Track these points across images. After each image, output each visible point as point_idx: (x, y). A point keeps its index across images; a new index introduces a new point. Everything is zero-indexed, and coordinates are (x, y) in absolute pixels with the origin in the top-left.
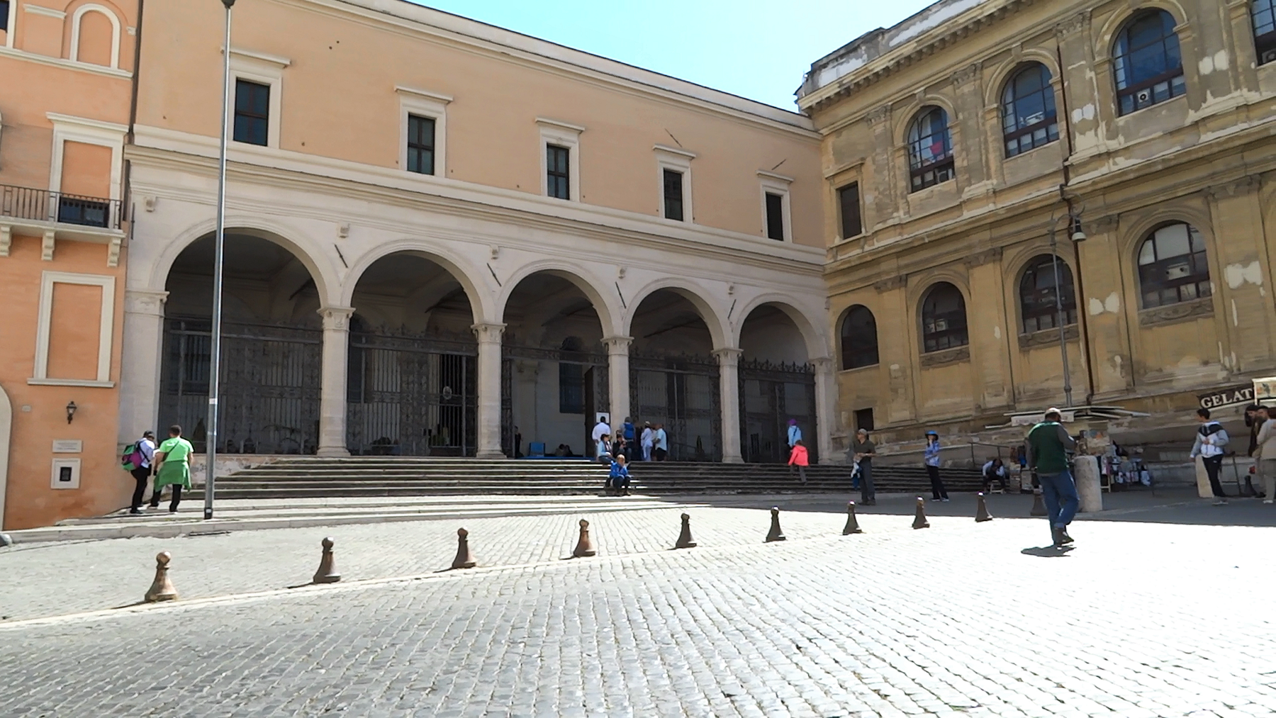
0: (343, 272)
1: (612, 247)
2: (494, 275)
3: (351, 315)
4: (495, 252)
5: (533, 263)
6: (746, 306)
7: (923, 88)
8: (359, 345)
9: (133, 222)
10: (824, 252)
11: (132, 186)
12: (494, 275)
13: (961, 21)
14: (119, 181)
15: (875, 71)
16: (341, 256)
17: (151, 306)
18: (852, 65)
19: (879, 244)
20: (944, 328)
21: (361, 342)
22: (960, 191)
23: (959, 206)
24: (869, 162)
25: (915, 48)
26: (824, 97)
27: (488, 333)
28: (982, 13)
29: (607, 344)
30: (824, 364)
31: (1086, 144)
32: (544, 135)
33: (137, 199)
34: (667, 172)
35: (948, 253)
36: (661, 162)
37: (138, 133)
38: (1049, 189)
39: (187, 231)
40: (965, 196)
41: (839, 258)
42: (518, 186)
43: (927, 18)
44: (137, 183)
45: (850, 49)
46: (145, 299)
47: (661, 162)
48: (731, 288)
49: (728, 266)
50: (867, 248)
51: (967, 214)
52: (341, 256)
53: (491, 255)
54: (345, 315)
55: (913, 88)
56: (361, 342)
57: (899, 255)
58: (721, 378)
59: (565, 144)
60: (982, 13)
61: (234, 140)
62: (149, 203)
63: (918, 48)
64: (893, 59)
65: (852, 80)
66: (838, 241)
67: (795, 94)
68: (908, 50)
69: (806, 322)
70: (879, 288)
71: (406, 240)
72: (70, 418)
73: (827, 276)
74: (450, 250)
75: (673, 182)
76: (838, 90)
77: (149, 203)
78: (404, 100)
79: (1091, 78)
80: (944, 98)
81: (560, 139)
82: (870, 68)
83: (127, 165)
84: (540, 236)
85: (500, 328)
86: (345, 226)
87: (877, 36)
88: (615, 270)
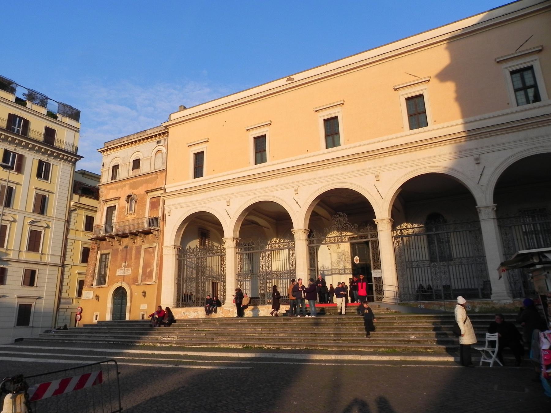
1: (369, 164)
2: (297, 203)
6: (496, 169)
12: (297, 203)
16: (228, 214)
33: (166, 212)
37: (167, 188)
46: (168, 249)
47: (402, 95)
48: (477, 159)
54: (230, 240)
62: (169, 213)
71: (255, 198)
72: (145, 296)
74: (275, 197)
81: (330, 114)
84: (321, 173)
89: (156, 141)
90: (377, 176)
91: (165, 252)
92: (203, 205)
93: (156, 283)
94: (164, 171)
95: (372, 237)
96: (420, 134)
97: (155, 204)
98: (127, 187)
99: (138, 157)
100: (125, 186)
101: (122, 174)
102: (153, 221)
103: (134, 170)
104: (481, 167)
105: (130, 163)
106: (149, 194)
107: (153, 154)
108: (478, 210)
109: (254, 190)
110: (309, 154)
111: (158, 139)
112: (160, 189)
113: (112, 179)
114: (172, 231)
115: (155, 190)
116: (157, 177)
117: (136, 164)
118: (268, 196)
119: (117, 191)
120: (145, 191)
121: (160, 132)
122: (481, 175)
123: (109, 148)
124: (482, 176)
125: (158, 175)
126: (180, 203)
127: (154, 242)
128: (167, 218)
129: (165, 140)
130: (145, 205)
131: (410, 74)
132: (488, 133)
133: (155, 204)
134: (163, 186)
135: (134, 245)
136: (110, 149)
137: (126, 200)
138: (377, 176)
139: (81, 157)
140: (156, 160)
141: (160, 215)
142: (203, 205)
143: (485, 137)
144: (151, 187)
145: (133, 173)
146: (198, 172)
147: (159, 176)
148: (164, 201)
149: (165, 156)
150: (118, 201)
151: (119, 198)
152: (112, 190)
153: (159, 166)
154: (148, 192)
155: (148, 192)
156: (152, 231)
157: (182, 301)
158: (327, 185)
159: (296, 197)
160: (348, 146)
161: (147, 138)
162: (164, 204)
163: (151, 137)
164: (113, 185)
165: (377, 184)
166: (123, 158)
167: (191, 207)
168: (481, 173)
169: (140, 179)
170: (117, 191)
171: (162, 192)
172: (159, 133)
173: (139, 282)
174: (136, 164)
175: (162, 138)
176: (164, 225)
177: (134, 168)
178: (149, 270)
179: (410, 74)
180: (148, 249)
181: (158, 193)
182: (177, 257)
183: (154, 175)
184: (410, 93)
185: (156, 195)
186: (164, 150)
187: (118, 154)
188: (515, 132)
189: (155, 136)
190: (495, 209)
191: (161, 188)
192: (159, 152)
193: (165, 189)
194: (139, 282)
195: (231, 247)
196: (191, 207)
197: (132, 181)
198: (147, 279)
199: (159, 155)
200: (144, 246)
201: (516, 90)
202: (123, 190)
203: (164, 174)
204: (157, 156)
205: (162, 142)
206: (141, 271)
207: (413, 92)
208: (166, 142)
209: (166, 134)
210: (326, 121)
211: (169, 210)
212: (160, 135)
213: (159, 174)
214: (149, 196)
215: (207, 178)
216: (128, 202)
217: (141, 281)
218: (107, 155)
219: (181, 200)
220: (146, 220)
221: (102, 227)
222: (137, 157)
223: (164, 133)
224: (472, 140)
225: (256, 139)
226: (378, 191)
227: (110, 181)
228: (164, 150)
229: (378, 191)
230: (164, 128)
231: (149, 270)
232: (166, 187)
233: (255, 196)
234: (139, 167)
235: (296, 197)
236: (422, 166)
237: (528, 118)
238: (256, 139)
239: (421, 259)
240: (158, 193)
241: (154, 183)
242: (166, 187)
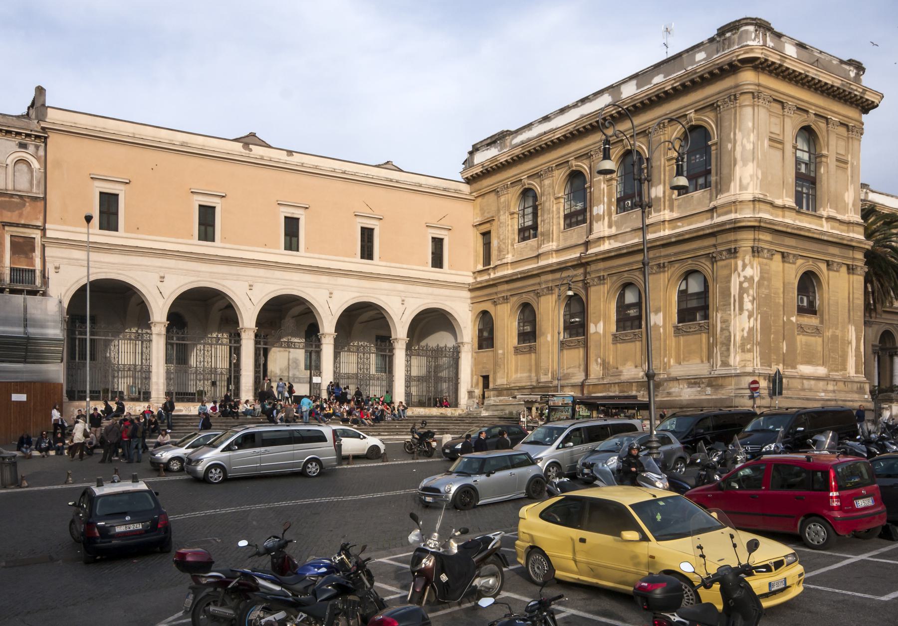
0: (161, 302)
1: (324, 279)
3: (167, 326)
4: (250, 286)
7: (526, 176)
8: (172, 341)
9: (48, 278)
10: (472, 274)
11: (46, 258)
13: (543, 139)
14: (40, 257)
15: (501, 161)
16: (161, 293)
18: (493, 152)
19: (500, 273)
20: (529, 330)
21: (173, 340)
22: (539, 247)
23: (538, 257)
24: (496, 220)
25: (521, 151)
26: (475, 173)
27: (247, 333)
28: (554, 136)
29: (321, 337)
31: (601, 229)
32: (282, 212)
33: (50, 267)
34: (363, 229)
35: (529, 286)
36: (359, 223)
38: (575, 254)
40: (541, 251)
41: (479, 279)
43: (531, 130)
44: (48, 257)
45: (492, 141)
49: (400, 286)
50: (492, 276)
51: (543, 262)
52: (161, 293)
55: (521, 175)
56: (173, 340)
57: (507, 282)
58: (394, 356)
60: (554, 136)
61: (100, 229)
62: (57, 268)
63: (523, 151)
64: (509, 156)
65: (488, 165)
66: (480, 267)
67: (463, 164)
68: (518, 151)
69: (455, 319)
70: (495, 303)
73: (471, 290)
74: (224, 286)
75: (367, 235)
76: (482, 169)
77: (56, 268)
78: (196, 197)
79: (604, 189)
80: (535, 184)
81: (293, 213)
82: (498, 159)
83: (44, 247)
84: (278, 274)
87: (505, 136)
90: (331, 293)
97: (23, 247)
104: (404, 306)
106: (7, 228)
107: (10, 161)
109: (199, 271)
111: (22, 139)
112: (37, 227)
115: (25, 226)
116: (24, 205)
118: (216, 283)
121: (33, 133)
125: (25, 201)
129: (37, 147)
133: (23, 247)
134: (39, 223)
138: (331, 293)
147: (27, 204)
159: (249, 292)
160: (308, 255)
165: (329, 300)
172: (29, 132)
175: (32, 144)
183: (16, 200)
185: (23, 233)
186: (35, 164)
189: (19, 134)
193: (44, 230)
199: (23, 167)
203: (41, 204)
205: (31, 149)
207: (367, 224)
212: (28, 135)
213: (27, 200)
223: (37, 137)
228: (35, 164)
230: (39, 129)
233: (199, 279)
235: (249, 292)
239: (123, 363)
241: (17, 213)
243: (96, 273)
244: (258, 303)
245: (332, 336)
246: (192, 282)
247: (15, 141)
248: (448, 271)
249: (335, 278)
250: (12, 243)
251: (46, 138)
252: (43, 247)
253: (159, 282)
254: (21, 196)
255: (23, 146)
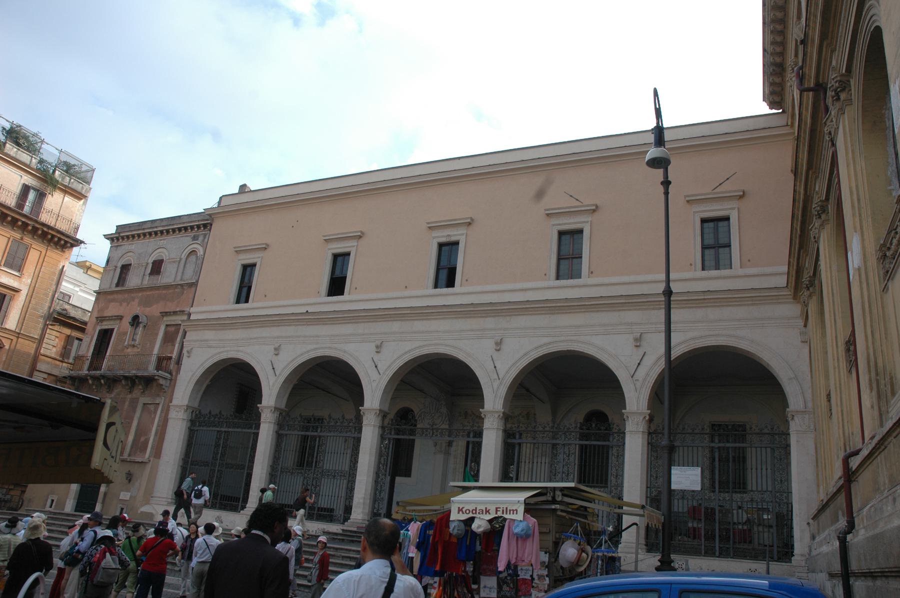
0: (272, 379)
1: (489, 322)
2: (376, 367)
5: (410, 351)
9: (181, 364)
12: (376, 367)
16: (273, 369)
17: (180, 413)
30: (795, 418)
33: (185, 351)
36: (554, 225)
39: (202, 365)
42: (406, 287)
53: (374, 349)
54: (270, 410)
59: (454, 239)
62: (188, 352)
71: (316, 349)
81: (449, 236)
84: (419, 325)
85: (375, 411)
86: (277, 346)
88: (489, 344)
89: (192, 235)
91: (173, 414)
92: (241, 348)
93: (150, 461)
94: (194, 285)
95: (474, 437)
96: (569, 290)
98: (137, 301)
99: (161, 255)
100: (133, 299)
101: (134, 280)
102: (162, 362)
103: (152, 277)
105: (148, 265)
106: (165, 319)
107: (184, 256)
108: (625, 417)
109: (318, 336)
110: (407, 293)
113: (117, 285)
114: (188, 383)
115: (175, 313)
116: (183, 293)
117: (157, 267)
119: (121, 305)
120: (161, 313)
122: (639, 364)
123: (121, 235)
124: (640, 366)
125: (184, 289)
126: (207, 340)
127: (158, 395)
128: (185, 361)
130: (157, 334)
131: (571, 196)
132: (658, 303)
134: (187, 309)
135: (129, 396)
136: (123, 238)
137: (130, 323)
139: (82, 242)
140: (187, 266)
141: (174, 355)
142: (241, 348)
143: (653, 309)
144: (171, 307)
145: (149, 279)
146: (244, 293)
147: (185, 292)
148: (186, 332)
149: (199, 262)
150: (118, 322)
151: (120, 318)
152: (113, 303)
153: (189, 277)
154: (165, 314)
155: (165, 314)
156: (157, 377)
157: (221, 500)
158: (424, 346)
161: (180, 229)
162: (184, 338)
163: (186, 229)
164: (115, 296)
166: (139, 254)
167: (222, 350)
168: (639, 362)
169: (157, 292)
170: (121, 305)
171: (185, 318)
173: (125, 456)
174: (157, 267)
175: (202, 232)
176: (178, 370)
177: (151, 274)
178: (142, 439)
179: (571, 196)
180: (148, 406)
181: (177, 319)
182: (189, 424)
184: (565, 224)
185: (174, 321)
186: (201, 252)
187: (133, 247)
188: (692, 307)
189: (192, 228)
190: (647, 418)
191: (184, 311)
192: (193, 253)
193: (189, 315)
194: (125, 456)
195: (268, 421)
196: (222, 350)
197: (145, 293)
198: (138, 453)
199: (193, 258)
200: (143, 400)
201: (704, 247)
202: (129, 305)
203: (193, 289)
204: (190, 259)
205: (201, 238)
206: (131, 438)
208: (206, 240)
209: (208, 228)
210: (441, 245)
211: (189, 349)
212: (199, 227)
214: (164, 321)
215: (256, 306)
216: (132, 325)
217: (129, 455)
218: (117, 246)
219: (209, 335)
220: (154, 359)
221: (88, 359)
222: (159, 256)
223: (205, 226)
224: (635, 310)
225: (336, 256)
226: (495, 367)
227: (114, 288)
229: (495, 367)
231: (142, 439)
232: (192, 310)
234: (160, 272)
236: (563, 338)
237: (709, 291)
238: (336, 256)
240: (177, 319)
242: (192, 310)
243: (219, 353)
244: (386, 370)
245: (496, 415)
246: (308, 351)
247: (191, 236)
248: (741, 272)
249: (508, 318)
250: (166, 333)
251: (211, 225)
252: (185, 333)
253: (274, 355)
254: (182, 285)
255: (195, 238)
